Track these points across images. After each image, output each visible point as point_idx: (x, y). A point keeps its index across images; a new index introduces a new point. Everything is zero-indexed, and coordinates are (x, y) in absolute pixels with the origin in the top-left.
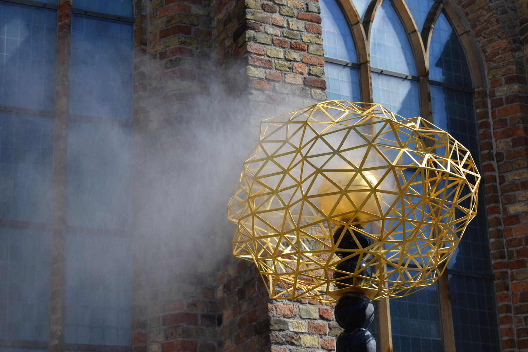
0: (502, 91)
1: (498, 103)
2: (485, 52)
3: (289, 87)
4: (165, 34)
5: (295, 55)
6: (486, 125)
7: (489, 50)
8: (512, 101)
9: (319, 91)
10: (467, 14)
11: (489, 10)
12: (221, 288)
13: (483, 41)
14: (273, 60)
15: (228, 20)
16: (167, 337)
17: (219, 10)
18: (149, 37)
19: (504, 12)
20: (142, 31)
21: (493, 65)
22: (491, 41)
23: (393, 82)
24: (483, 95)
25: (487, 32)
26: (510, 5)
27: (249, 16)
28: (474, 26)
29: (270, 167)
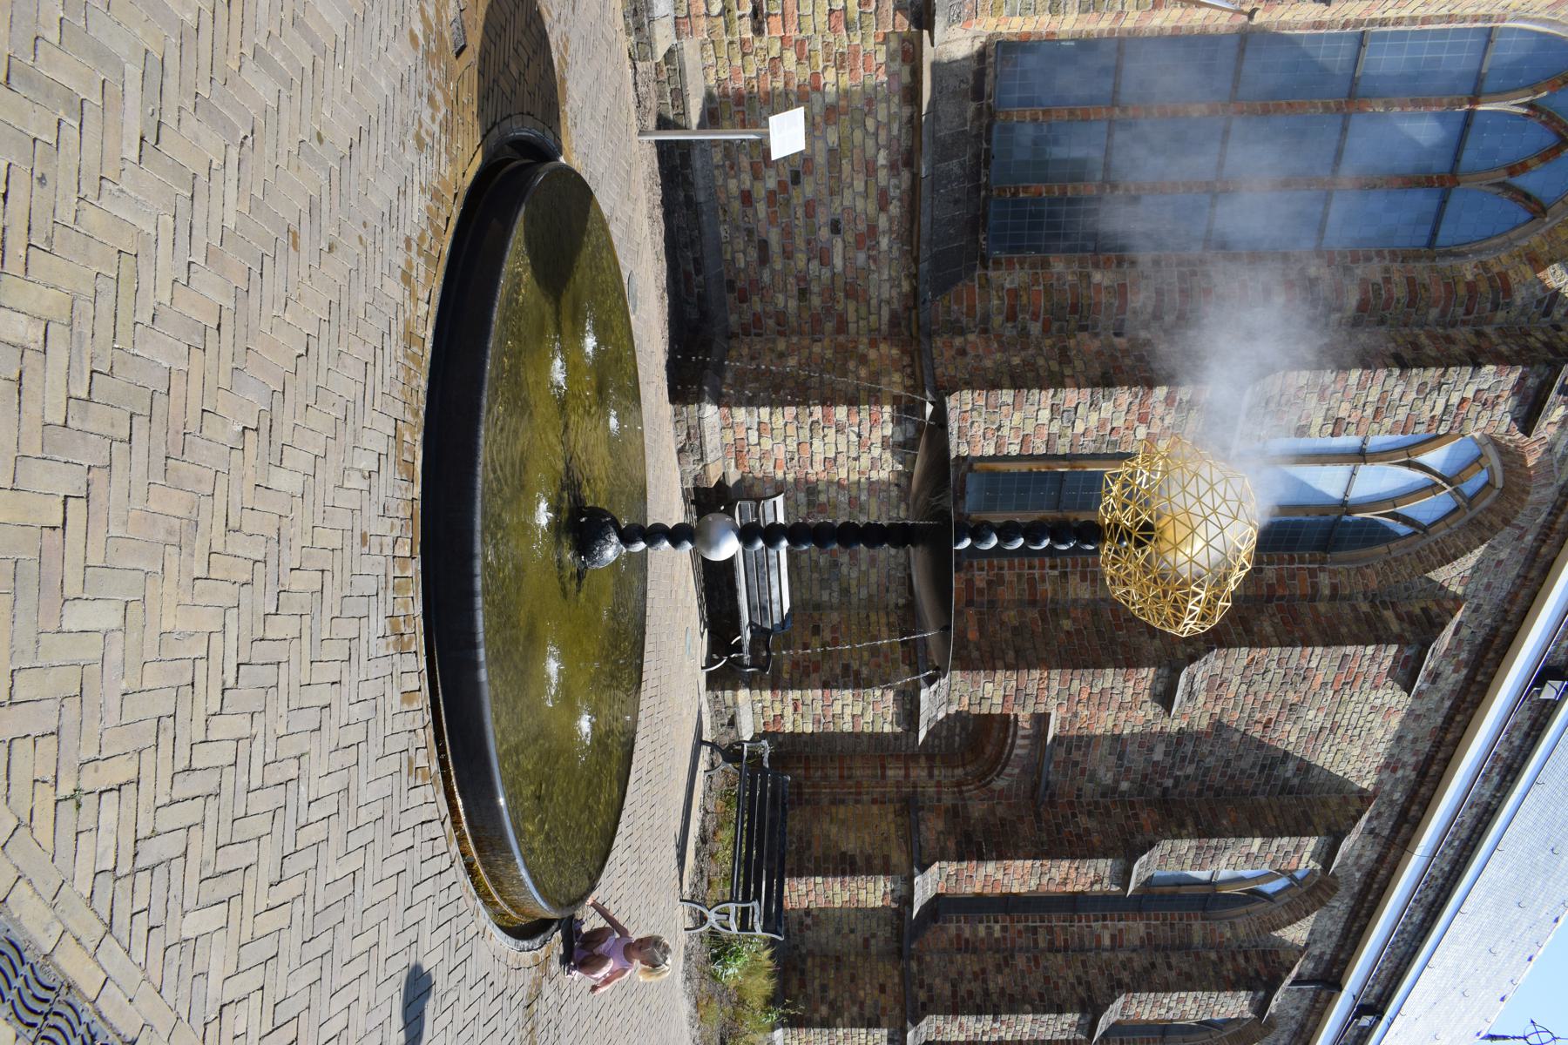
0: (1324, 580)
1: (1313, 574)
2: (1367, 567)
3: (1336, 405)
4: (1411, 282)
5: (1369, 411)
6: (1292, 561)
7: (1368, 571)
8: (1312, 587)
9: (1330, 431)
10: (1409, 554)
11: (1410, 576)
12: (1149, 336)
13: (1379, 567)
14: (1365, 392)
15: (1416, 346)
16: (1106, 288)
17: (1430, 336)
18: (1411, 265)
19: (1406, 589)
20: (1417, 257)
21: (1352, 573)
22: (1377, 574)
23: (1343, 485)
24: (1323, 561)
25: (1388, 571)
26: (1414, 595)
27: (1415, 371)
28: (1396, 560)
29: (1204, 487)
